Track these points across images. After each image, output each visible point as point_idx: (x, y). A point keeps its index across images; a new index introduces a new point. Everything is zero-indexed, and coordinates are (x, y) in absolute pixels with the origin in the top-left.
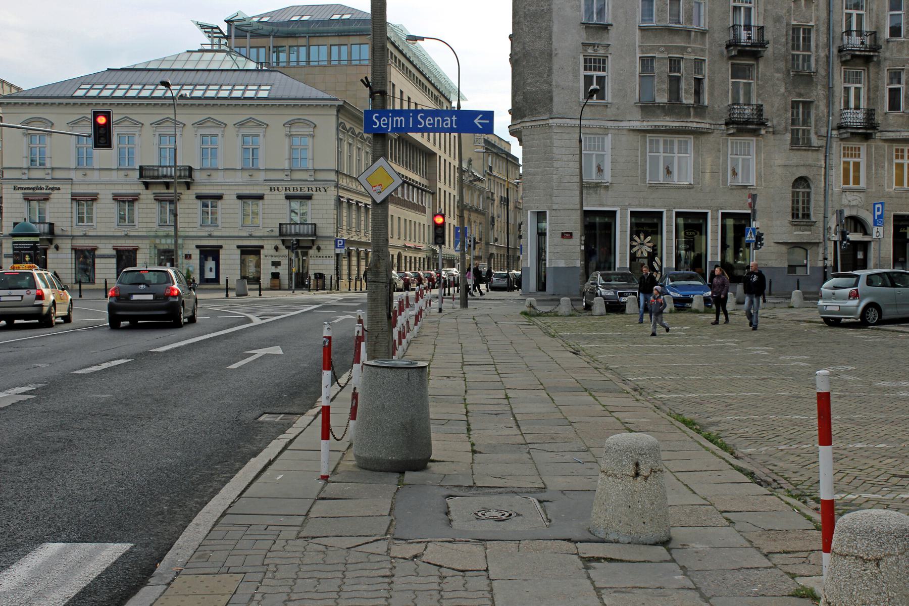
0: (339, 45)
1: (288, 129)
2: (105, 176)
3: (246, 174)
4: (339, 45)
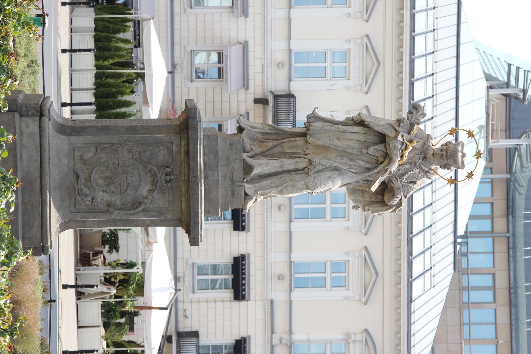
0: (492, 217)
1: (359, 337)
2: (278, 29)
3: (284, 270)
4: (494, 288)
